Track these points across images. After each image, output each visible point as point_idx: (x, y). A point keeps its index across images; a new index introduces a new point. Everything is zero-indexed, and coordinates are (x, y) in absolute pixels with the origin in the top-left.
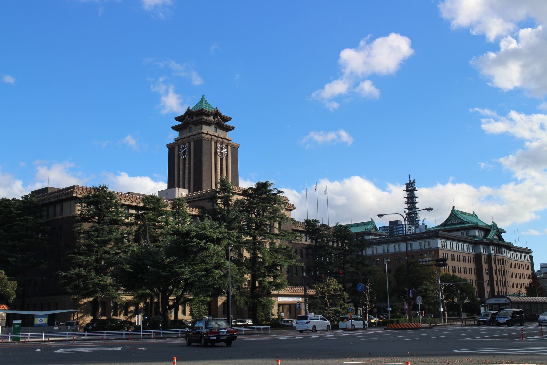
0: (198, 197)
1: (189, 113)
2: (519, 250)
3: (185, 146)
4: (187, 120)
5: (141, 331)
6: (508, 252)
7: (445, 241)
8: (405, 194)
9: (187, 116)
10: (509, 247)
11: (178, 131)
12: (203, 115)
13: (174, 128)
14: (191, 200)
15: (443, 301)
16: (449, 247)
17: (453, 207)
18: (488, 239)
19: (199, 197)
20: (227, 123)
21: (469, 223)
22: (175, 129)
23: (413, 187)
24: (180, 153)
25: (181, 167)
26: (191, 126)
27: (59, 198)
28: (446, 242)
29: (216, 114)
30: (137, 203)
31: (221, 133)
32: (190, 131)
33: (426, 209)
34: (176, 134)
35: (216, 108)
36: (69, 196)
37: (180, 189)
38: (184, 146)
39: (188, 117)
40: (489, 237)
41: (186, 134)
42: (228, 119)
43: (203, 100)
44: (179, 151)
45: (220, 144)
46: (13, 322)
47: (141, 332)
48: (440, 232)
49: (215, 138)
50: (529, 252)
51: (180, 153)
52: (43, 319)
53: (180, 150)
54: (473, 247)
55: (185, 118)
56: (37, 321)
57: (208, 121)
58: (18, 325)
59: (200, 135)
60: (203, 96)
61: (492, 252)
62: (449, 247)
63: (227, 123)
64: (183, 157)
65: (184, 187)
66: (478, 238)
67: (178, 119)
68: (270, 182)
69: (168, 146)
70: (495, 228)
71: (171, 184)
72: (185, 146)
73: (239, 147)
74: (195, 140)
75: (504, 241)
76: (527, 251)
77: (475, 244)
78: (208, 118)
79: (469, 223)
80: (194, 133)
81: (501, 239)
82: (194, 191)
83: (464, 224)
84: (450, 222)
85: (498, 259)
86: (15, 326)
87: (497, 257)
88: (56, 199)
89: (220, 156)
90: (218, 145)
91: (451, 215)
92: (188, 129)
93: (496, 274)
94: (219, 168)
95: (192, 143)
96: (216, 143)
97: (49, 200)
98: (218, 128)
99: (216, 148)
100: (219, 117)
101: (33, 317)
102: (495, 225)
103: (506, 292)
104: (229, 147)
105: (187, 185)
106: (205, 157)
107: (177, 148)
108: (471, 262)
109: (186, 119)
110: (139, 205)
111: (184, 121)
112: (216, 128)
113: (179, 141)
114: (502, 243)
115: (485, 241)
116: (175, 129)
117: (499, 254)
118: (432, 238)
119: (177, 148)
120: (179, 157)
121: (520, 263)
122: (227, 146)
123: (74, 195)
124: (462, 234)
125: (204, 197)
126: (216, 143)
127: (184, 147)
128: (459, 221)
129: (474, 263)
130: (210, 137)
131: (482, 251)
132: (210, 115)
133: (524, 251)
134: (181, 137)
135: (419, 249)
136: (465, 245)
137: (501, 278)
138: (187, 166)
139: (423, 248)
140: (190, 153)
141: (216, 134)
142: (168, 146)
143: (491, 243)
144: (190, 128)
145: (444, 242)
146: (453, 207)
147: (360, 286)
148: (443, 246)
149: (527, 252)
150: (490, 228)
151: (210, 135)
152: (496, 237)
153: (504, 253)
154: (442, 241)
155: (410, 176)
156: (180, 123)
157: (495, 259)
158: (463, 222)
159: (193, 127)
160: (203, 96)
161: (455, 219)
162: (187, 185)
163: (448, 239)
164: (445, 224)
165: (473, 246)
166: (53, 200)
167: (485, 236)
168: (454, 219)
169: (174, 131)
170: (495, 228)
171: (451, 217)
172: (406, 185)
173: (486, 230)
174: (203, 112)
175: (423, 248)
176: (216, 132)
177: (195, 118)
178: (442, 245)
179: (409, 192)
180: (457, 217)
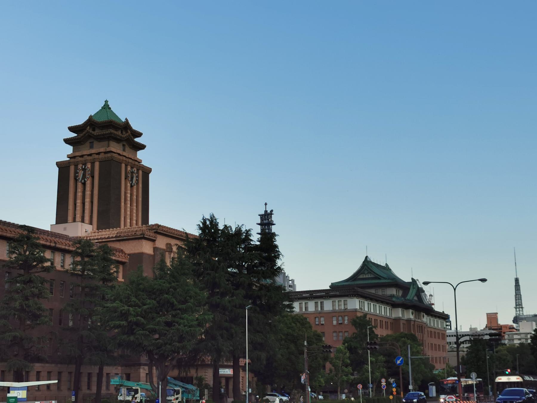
0: (115, 237)
1: (91, 122)
2: (437, 315)
3: (85, 167)
4: (88, 132)
7: (363, 301)
9: (88, 127)
11: (71, 145)
12: (111, 128)
13: (67, 141)
14: (104, 240)
16: (366, 309)
17: (367, 257)
18: (408, 300)
19: (116, 237)
20: (137, 140)
21: (385, 278)
22: (67, 142)
23: (270, 220)
24: (77, 175)
25: (79, 194)
28: (364, 302)
29: (126, 126)
31: (128, 153)
32: (91, 147)
33: (480, 280)
34: (69, 149)
35: (126, 119)
37: (83, 224)
38: (84, 166)
39: (90, 129)
40: (408, 297)
41: (85, 151)
42: (139, 135)
43: (106, 107)
44: (76, 172)
45: (131, 167)
46: (8, 396)
50: (446, 317)
51: (77, 175)
52: (20, 392)
53: (78, 171)
54: (390, 309)
55: (86, 130)
57: (118, 137)
58: (14, 400)
60: (106, 102)
62: (366, 309)
63: (137, 140)
64: (81, 181)
67: (71, 129)
68: (276, 233)
69: (58, 164)
70: (415, 287)
71: (61, 217)
72: (85, 167)
73: (151, 171)
74: (101, 160)
75: (424, 304)
76: (443, 316)
78: (116, 132)
79: (385, 278)
83: (379, 279)
84: (361, 277)
85: (417, 326)
86: (10, 400)
87: (416, 323)
89: (131, 183)
90: (129, 168)
92: (88, 144)
95: (97, 165)
98: (127, 146)
101: (8, 389)
102: (415, 283)
105: (87, 218)
107: (72, 168)
108: (383, 328)
109: (86, 131)
110: (57, 246)
111: (84, 133)
112: (124, 145)
116: (67, 142)
117: (418, 319)
118: (349, 296)
120: (76, 180)
121: (437, 331)
122: (138, 170)
125: (124, 238)
126: (126, 166)
127: (83, 167)
128: (372, 276)
129: (391, 330)
132: (119, 129)
134: (78, 154)
135: (332, 309)
138: (88, 193)
139: (337, 309)
140: (93, 177)
141: (125, 154)
142: (58, 164)
144: (92, 143)
145: (362, 301)
147: (399, 360)
148: (361, 307)
149: (445, 317)
151: (119, 154)
152: (416, 298)
153: (423, 317)
154: (360, 301)
155: (266, 204)
156: (74, 135)
157: (414, 325)
158: (378, 277)
160: (106, 102)
161: (368, 273)
162: (87, 218)
164: (354, 277)
165: (391, 308)
169: (66, 144)
170: (415, 287)
171: (364, 270)
172: (261, 217)
174: (112, 124)
175: (337, 309)
177: (97, 132)
179: (263, 227)
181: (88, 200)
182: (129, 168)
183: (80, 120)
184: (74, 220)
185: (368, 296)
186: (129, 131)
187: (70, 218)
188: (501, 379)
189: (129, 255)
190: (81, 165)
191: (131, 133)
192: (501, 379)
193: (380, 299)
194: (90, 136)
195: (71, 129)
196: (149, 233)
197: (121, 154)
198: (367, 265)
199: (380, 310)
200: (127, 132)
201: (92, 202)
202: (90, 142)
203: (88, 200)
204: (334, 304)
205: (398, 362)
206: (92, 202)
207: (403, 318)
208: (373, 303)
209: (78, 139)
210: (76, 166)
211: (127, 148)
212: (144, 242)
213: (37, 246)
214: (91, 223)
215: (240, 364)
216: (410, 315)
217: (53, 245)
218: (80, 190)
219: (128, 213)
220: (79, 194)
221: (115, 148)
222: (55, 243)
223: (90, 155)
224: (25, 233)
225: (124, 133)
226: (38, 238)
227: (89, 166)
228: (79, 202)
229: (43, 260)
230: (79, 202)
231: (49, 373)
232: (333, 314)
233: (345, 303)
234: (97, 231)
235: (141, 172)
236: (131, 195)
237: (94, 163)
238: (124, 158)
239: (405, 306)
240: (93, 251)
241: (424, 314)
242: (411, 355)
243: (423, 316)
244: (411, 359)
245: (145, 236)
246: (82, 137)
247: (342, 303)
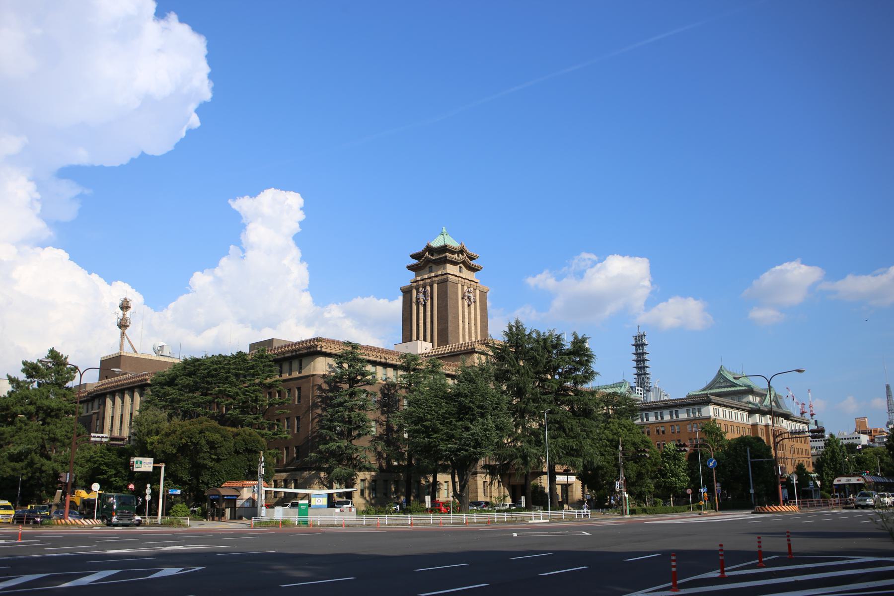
2: (797, 419)
5: (451, 515)
6: (785, 421)
8: (633, 349)
9: (427, 253)
13: (410, 268)
14: (440, 356)
18: (765, 406)
19: (451, 352)
20: (473, 262)
21: (740, 386)
25: (421, 315)
26: (430, 265)
27: (298, 353)
30: (386, 359)
31: (466, 274)
32: (431, 271)
34: (412, 275)
36: (312, 350)
40: (765, 403)
47: (451, 516)
48: (712, 397)
50: (808, 422)
56: (315, 501)
59: (445, 277)
63: (473, 262)
66: (753, 404)
67: (414, 257)
71: (407, 337)
78: (453, 256)
79: (740, 386)
83: (735, 386)
88: (294, 353)
90: (466, 288)
92: (427, 269)
94: (466, 317)
95: (435, 286)
97: (284, 354)
98: (463, 267)
100: (465, 255)
104: (478, 291)
106: (450, 303)
107: (414, 292)
112: (460, 267)
119: (414, 292)
120: (418, 303)
123: (319, 349)
125: (458, 353)
126: (463, 286)
128: (728, 384)
130: (457, 278)
133: (802, 421)
140: (432, 299)
141: (461, 275)
146: (721, 367)
150: (766, 393)
151: (456, 276)
154: (714, 408)
156: (415, 262)
159: (434, 267)
163: (720, 405)
164: (710, 387)
166: (289, 355)
167: (762, 402)
178: (714, 413)
180: (726, 378)
181: (429, 320)
182: (466, 288)
183: (419, 249)
184: (418, 339)
185: (722, 403)
186: (465, 254)
187: (414, 338)
188: (840, 481)
190: (421, 288)
191: (467, 256)
192: (840, 481)
193: (736, 406)
194: (428, 261)
195: (414, 257)
196: (481, 347)
197: (458, 275)
199: (737, 417)
200: (463, 255)
202: (429, 267)
203: (429, 320)
204: (689, 412)
205: (711, 464)
207: (761, 424)
208: (722, 409)
209: (418, 264)
212: (476, 355)
213: (362, 361)
215: (556, 471)
216: (767, 420)
217: (383, 360)
219: (467, 330)
220: (421, 315)
221: (450, 269)
222: (385, 358)
223: (430, 278)
224: (350, 349)
225: (460, 255)
226: (361, 354)
227: (428, 288)
229: (364, 375)
231: (285, 481)
232: (689, 421)
233: (694, 412)
234: (438, 347)
235: (478, 291)
236: (469, 313)
237: (432, 285)
239: (763, 413)
240: (421, 364)
241: (783, 419)
242: (751, 458)
243: (782, 421)
244: (752, 463)
245: (476, 350)
246: (421, 262)
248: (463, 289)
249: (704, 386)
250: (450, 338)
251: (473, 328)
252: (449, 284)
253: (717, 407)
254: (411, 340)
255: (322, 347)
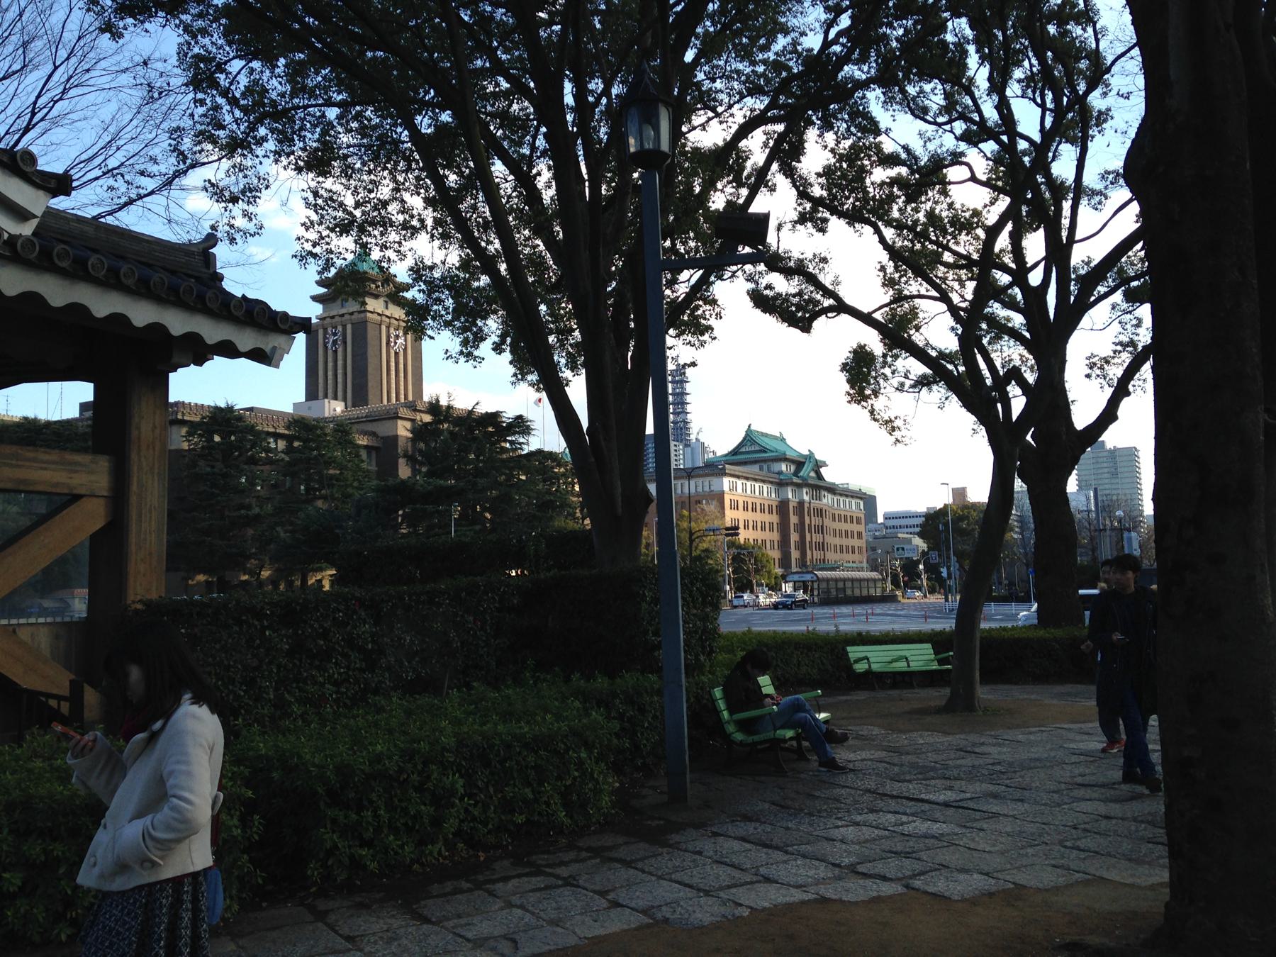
6: (830, 496)
10: (832, 489)
13: (315, 298)
15: (729, 575)
16: (739, 490)
19: (366, 417)
25: (330, 365)
40: (801, 474)
41: (336, 310)
44: (325, 338)
49: (387, 320)
59: (362, 315)
61: (806, 498)
62: (739, 490)
65: (336, 398)
66: (786, 475)
71: (312, 392)
77: (781, 484)
80: (351, 310)
81: (820, 477)
82: (354, 406)
83: (765, 452)
84: (743, 450)
90: (392, 330)
91: (744, 439)
92: (339, 302)
93: (810, 531)
94: (393, 368)
95: (349, 327)
96: (388, 327)
99: (388, 337)
103: (824, 560)
105: (340, 394)
106: (371, 351)
112: (386, 302)
113: (326, 322)
114: (821, 483)
115: (796, 480)
120: (326, 348)
121: (849, 514)
123: (180, 417)
124: (761, 469)
126: (388, 327)
130: (379, 318)
131: (790, 496)
136: (765, 487)
137: (817, 538)
138: (340, 363)
140: (345, 342)
143: (804, 484)
151: (379, 314)
152: (813, 474)
156: (322, 290)
157: (809, 508)
158: (764, 450)
162: (340, 394)
163: (738, 477)
164: (735, 452)
167: (796, 474)
168: (749, 444)
173: (799, 464)
176: (387, 308)
181: (340, 371)
184: (326, 396)
187: (321, 394)
189: (382, 438)
198: (750, 437)
201: (345, 374)
203: (340, 371)
206: (345, 374)
210: (325, 330)
211: (391, 306)
212: (400, 422)
214: (345, 400)
218: (330, 359)
219: (393, 386)
220: (330, 365)
227: (340, 328)
228: (330, 373)
230: (330, 373)
238: (384, 318)
247: (706, 484)
248: (388, 331)
249: (726, 452)
250: (371, 397)
251: (402, 383)
252: (370, 326)
253: (734, 480)
254: (316, 398)
255: (183, 414)
